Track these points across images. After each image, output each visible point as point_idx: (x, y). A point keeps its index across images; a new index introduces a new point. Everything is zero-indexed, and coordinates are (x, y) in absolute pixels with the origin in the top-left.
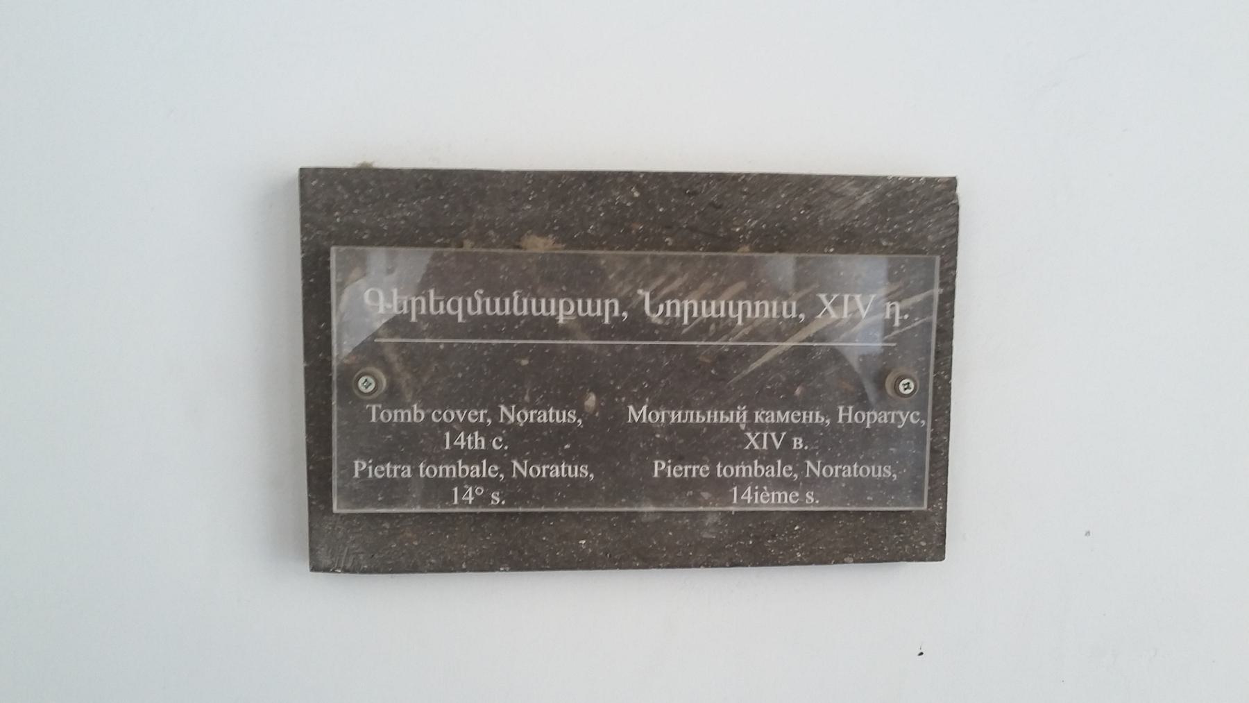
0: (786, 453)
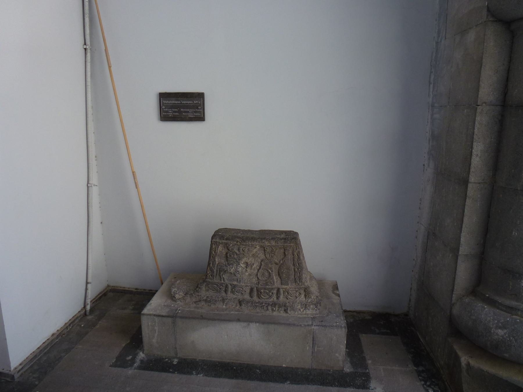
0: (192, 113)
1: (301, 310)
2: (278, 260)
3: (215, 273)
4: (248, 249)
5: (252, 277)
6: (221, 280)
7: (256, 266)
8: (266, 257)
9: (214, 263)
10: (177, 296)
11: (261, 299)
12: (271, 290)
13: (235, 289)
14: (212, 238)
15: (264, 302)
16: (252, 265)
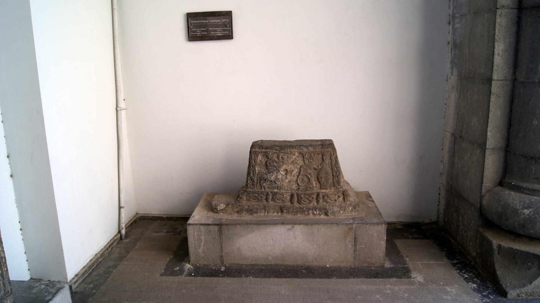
1: (341, 212)
2: (316, 166)
3: (256, 181)
4: (287, 156)
5: (292, 183)
6: (261, 189)
7: (295, 172)
8: (305, 163)
9: (254, 172)
10: (219, 208)
11: (301, 205)
12: (311, 195)
13: (276, 197)
14: (251, 148)
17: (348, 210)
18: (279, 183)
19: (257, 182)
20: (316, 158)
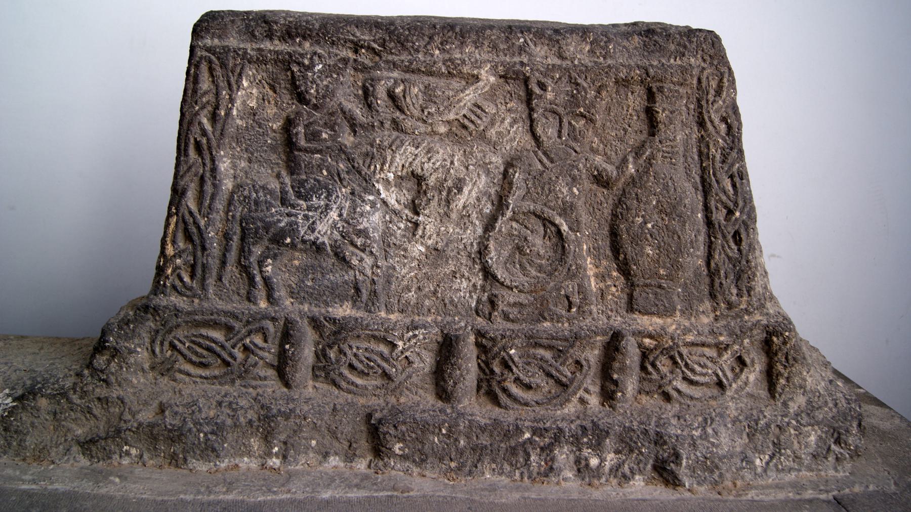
1: (758, 462)
2: (608, 159)
3: (215, 248)
6: (250, 298)
7: (474, 194)
9: (208, 188)
11: (506, 408)
12: (572, 346)
13: (341, 351)
15: (527, 424)
16: (449, 191)
17: (796, 446)
18: (369, 261)
19: (226, 249)
20: (608, 110)
